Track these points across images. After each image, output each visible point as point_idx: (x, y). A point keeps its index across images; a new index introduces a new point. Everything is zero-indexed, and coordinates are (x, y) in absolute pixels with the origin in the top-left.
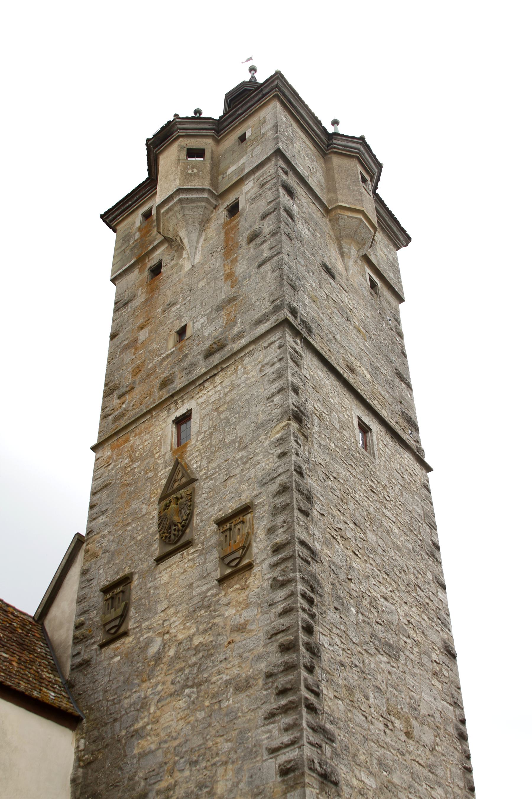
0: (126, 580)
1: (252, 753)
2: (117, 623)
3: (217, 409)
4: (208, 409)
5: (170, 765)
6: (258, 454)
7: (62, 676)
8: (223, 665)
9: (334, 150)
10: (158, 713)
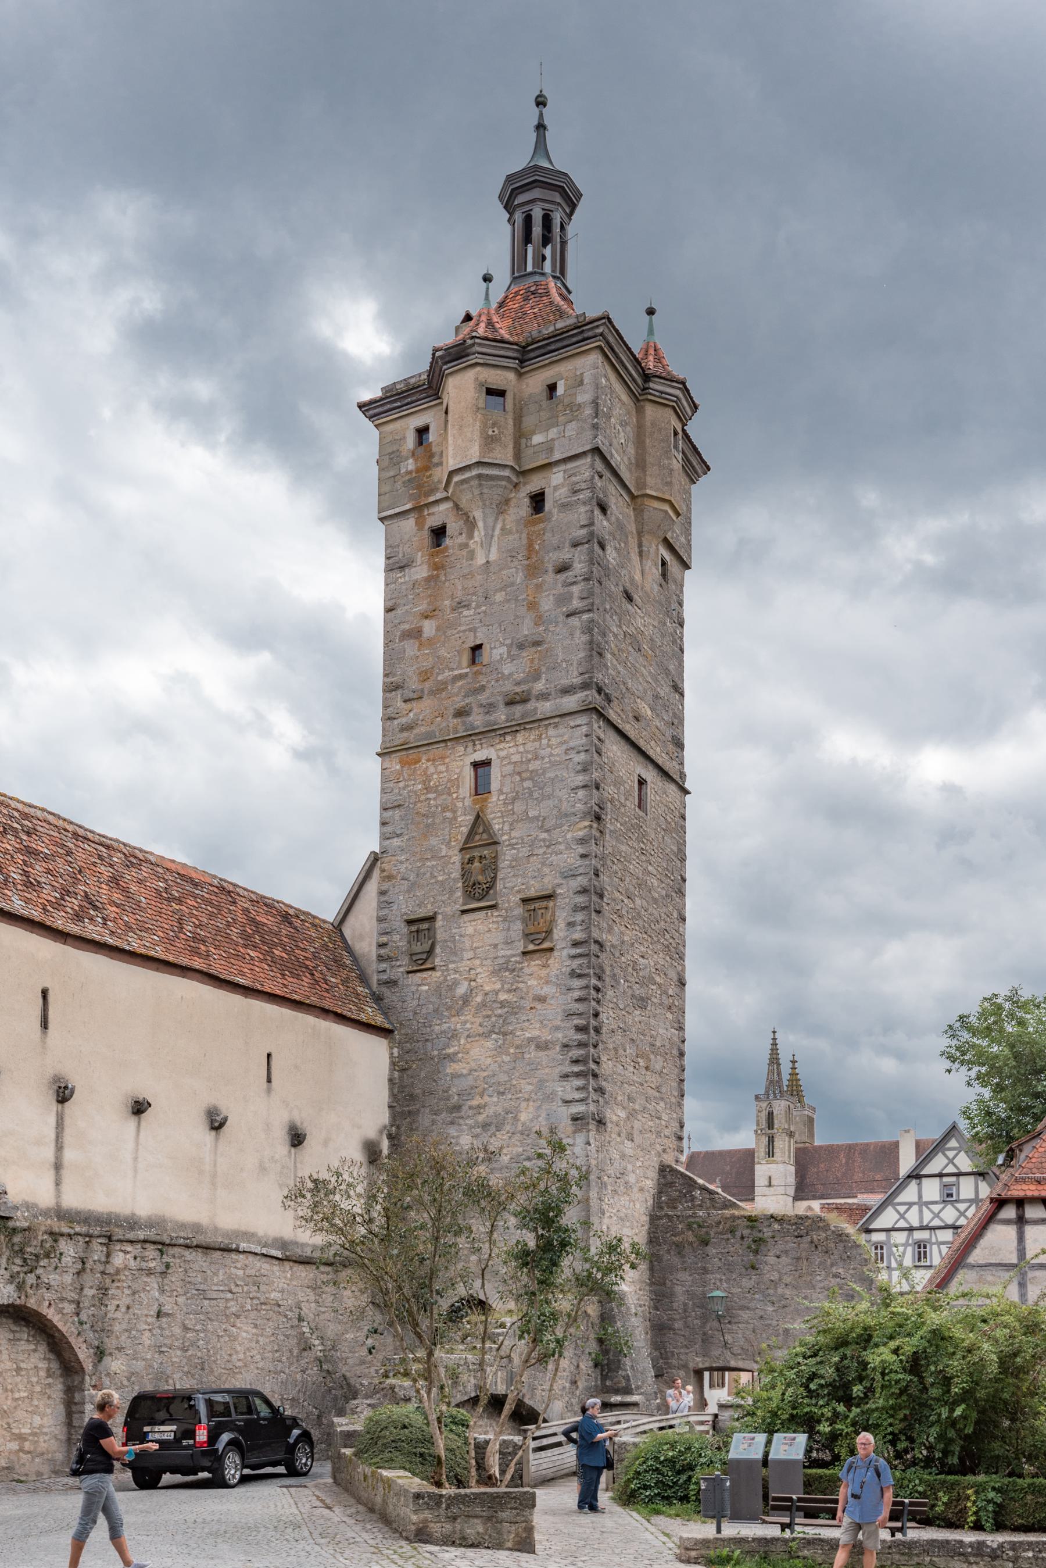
0: (431, 919)
1: (549, 1098)
2: (424, 956)
3: (519, 774)
4: (510, 768)
5: (480, 1089)
6: (560, 843)
7: (369, 987)
8: (526, 1024)
9: (650, 397)
10: (468, 1046)
